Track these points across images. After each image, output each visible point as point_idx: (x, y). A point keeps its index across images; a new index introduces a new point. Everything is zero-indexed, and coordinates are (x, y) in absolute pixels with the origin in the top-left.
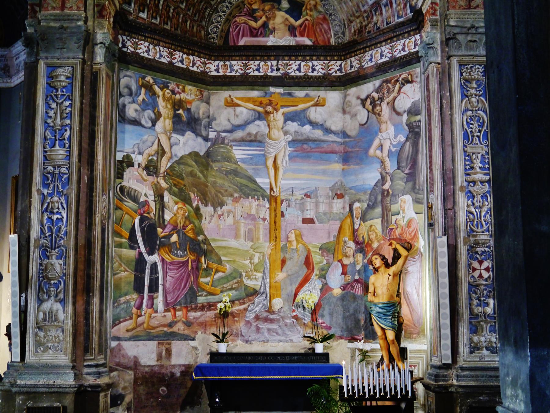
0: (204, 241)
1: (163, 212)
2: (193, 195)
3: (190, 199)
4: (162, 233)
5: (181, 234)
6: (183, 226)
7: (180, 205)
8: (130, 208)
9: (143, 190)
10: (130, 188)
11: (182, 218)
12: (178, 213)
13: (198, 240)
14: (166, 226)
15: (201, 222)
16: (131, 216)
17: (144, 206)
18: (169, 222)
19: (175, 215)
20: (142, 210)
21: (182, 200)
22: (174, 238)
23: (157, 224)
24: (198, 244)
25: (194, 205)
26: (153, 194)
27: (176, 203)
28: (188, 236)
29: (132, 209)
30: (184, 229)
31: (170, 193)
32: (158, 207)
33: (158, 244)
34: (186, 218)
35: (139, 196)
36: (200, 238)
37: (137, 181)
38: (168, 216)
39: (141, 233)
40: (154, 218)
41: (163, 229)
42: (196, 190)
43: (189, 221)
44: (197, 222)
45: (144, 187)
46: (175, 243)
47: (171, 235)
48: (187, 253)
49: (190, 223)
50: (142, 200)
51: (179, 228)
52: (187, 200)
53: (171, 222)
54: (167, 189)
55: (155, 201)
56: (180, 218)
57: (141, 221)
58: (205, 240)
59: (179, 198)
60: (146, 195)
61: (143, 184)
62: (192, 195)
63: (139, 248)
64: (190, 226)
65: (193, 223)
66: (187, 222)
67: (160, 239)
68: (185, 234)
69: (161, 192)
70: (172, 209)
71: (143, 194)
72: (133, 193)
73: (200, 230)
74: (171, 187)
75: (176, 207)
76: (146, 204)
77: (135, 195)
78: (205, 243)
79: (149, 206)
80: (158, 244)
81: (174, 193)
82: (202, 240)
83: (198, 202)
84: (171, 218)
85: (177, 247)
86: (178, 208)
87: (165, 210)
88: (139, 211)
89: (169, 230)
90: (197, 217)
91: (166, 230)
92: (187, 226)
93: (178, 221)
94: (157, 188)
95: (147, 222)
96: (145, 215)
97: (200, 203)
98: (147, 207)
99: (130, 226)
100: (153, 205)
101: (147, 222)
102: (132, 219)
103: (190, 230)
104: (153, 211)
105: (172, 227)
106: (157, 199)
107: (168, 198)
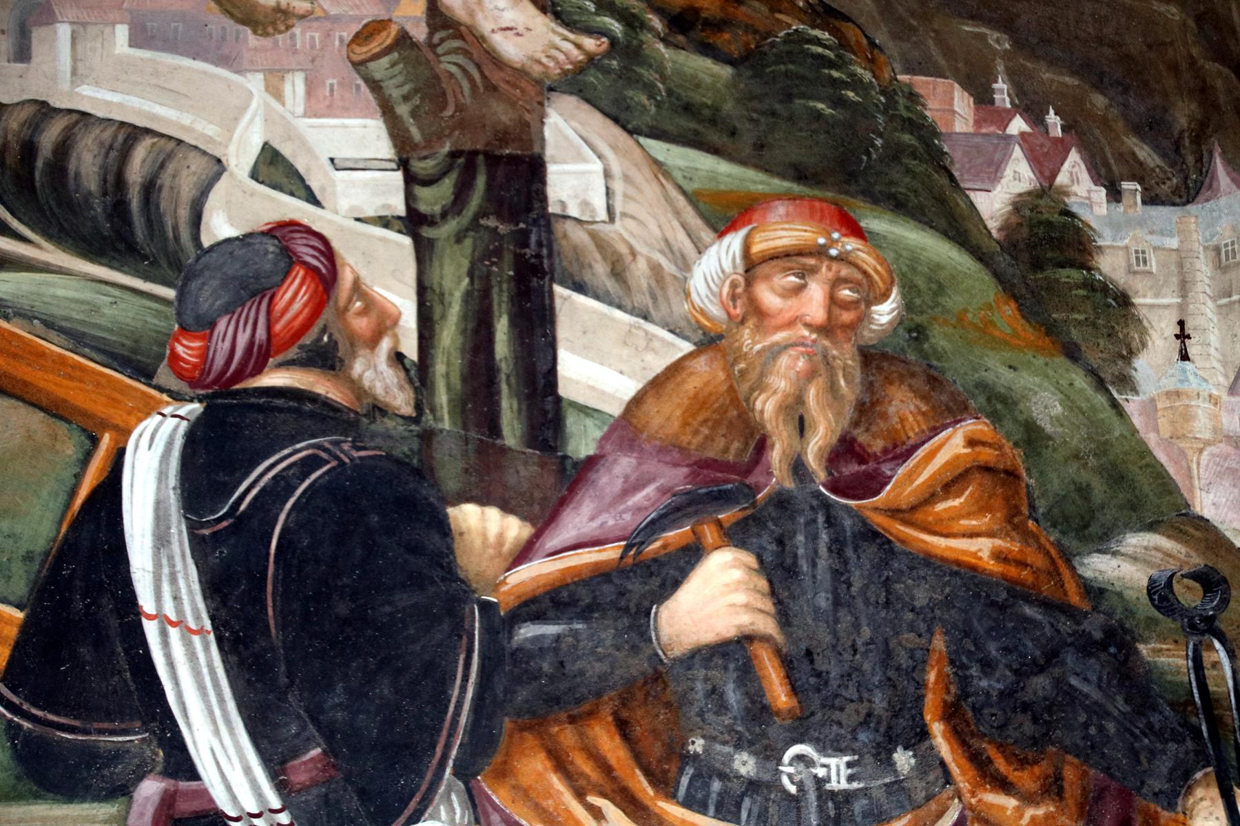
0: (1189, 596)
1: (537, 326)
2: (962, 103)
3: (927, 142)
4: (523, 554)
5: (812, 548)
6: (845, 449)
7: (783, 230)
8: (49, 324)
9: (230, 121)
10: (44, 111)
11: (821, 367)
12: (757, 311)
13: (1095, 592)
14: (575, 476)
15: (1113, 378)
16: (55, 410)
17: (254, 290)
18: (627, 428)
19: (709, 341)
20: (232, 337)
21: (800, 175)
22: (717, 598)
23: (450, 467)
24: (1087, 646)
25: (993, 204)
26: (383, 148)
27: (724, 212)
28: (929, 560)
29: (77, 338)
30: (869, 484)
31: (620, 115)
32: (454, 278)
33: (464, 694)
34: (870, 357)
35: (183, 180)
36: (1126, 565)
37: (140, 38)
38: (601, 362)
39: (216, 587)
40: (402, 401)
41: (544, 517)
42: (999, 41)
43: (933, 382)
44: (1048, 393)
45: (255, 83)
46: (733, 652)
47: (672, 572)
48: (930, 763)
49: (950, 410)
50: (220, 225)
51: (776, 472)
52: (872, 166)
53: (664, 417)
54: (575, 82)
55: (413, 222)
56: (790, 366)
57: (207, 465)
58: (1208, 580)
59: (758, 157)
60: (274, 168)
61: (224, 61)
62: (952, 109)
63: (180, 764)
64: (952, 445)
65: (999, 405)
66: (903, 406)
67: (500, 623)
68: (870, 534)
69: (502, 114)
70: (669, 281)
71: (241, 157)
72: (87, 163)
73: (1117, 476)
74: (627, 52)
75: (722, 256)
76: (289, 259)
77: (116, 182)
78: (1203, 627)
79: (326, 274)
80: (464, 694)
81: (688, 109)
82: (1160, 593)
83: (1045, 161)
84: (657, 385)
85: (759, 711)
86: (752, 265)
87: (571, 307)
88: (186, 350)
89: (625, 518)
90: (1050, 329)
91: (577, 521)
92: (900, 452)
93: (767, 406)
94: (431, 91)
95: (302, 449)
96: (274, 379)
97: (1075, 176)
98: (294, 297)
99: (40, 523)
100: (385, 273)
101: (302, 449)
102: (70, 448)
103: (950, 484)
104: (386, 323)
105: (675, 477)
106: (432, 199)
107: (583, 167)
